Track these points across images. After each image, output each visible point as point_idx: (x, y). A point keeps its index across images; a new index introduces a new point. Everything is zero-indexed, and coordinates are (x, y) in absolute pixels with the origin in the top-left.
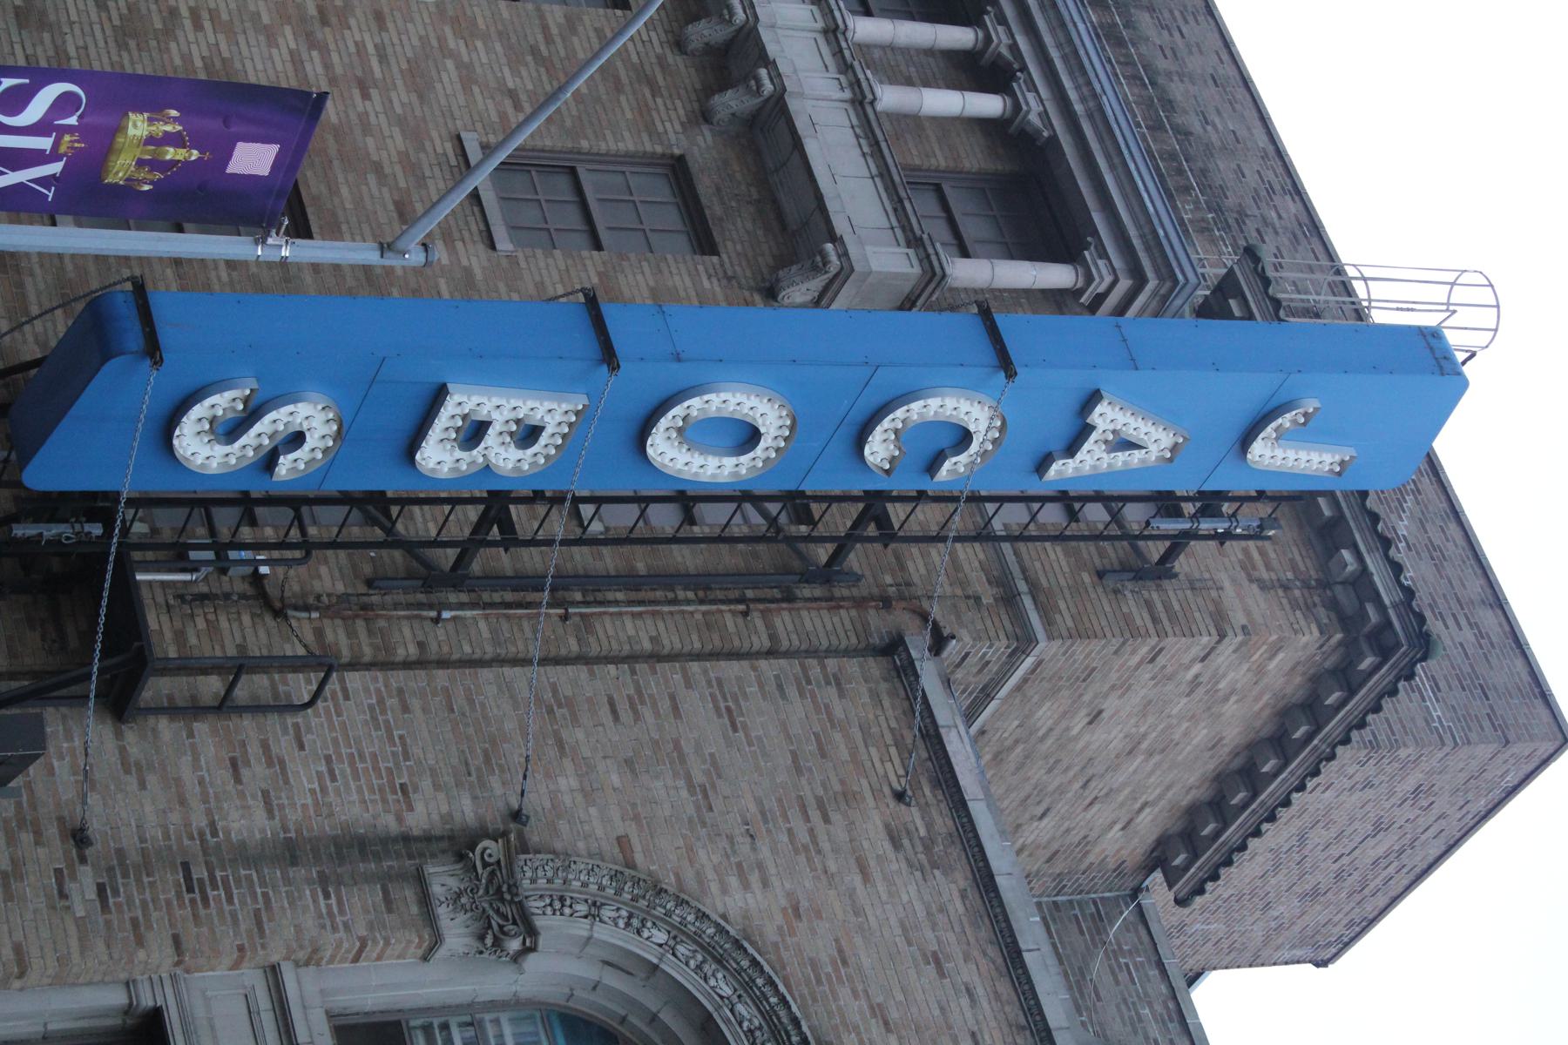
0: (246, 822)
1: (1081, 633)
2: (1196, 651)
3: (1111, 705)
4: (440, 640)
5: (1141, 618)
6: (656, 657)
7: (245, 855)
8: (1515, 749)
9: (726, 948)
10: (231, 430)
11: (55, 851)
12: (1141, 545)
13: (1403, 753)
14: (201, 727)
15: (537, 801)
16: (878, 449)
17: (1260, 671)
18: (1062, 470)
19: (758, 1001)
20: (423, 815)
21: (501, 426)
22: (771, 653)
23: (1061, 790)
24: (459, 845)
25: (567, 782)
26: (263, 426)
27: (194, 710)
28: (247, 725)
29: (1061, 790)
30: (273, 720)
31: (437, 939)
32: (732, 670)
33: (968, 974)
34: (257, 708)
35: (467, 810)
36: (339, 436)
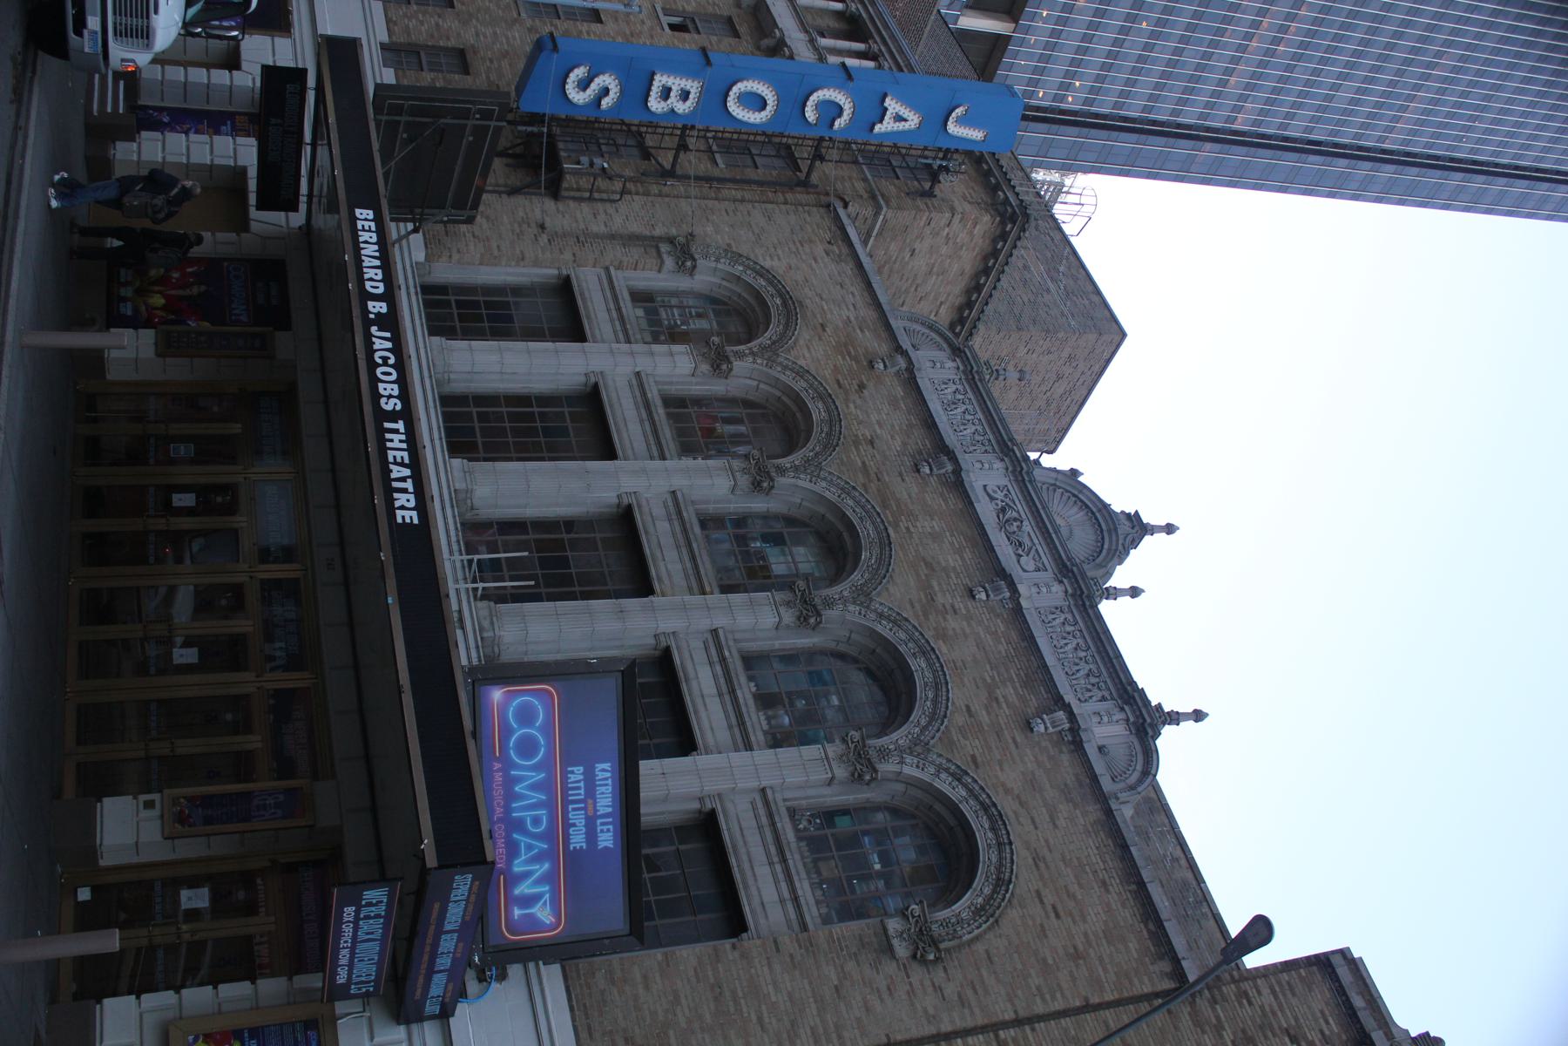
0: (598, 227)
1: (899, 208)
2: (944, 222)
3: (917, 246)
4: (666, 190)
5: (923, 206)
6: (742, 201)
7: (597, 236)
8: (1104, 338)
9: (763, 272)
10: (584, 85)
11: (534, 230)
12: (919, 170)
13: (1061, 335)
14: (585, 207)
15: (698, 230)
16: (810, 115)
17: (971, 233)
18: (878, 128)
19: (775, 287)
20: (658, 232)
21: (675, 94)
22: (786, 203)
23: (907, 291)
24: (671, 240)
25: (709, 229)
26: (594, 86)
27: (581, 200)
28: (599, 205)
29: (907, 291)
30: (608, 205)
31: (662, 262)
32: (770, 206)
33: (852, 289)
34: (602, 200)
35: (674, 232)
36: (621, 91)
